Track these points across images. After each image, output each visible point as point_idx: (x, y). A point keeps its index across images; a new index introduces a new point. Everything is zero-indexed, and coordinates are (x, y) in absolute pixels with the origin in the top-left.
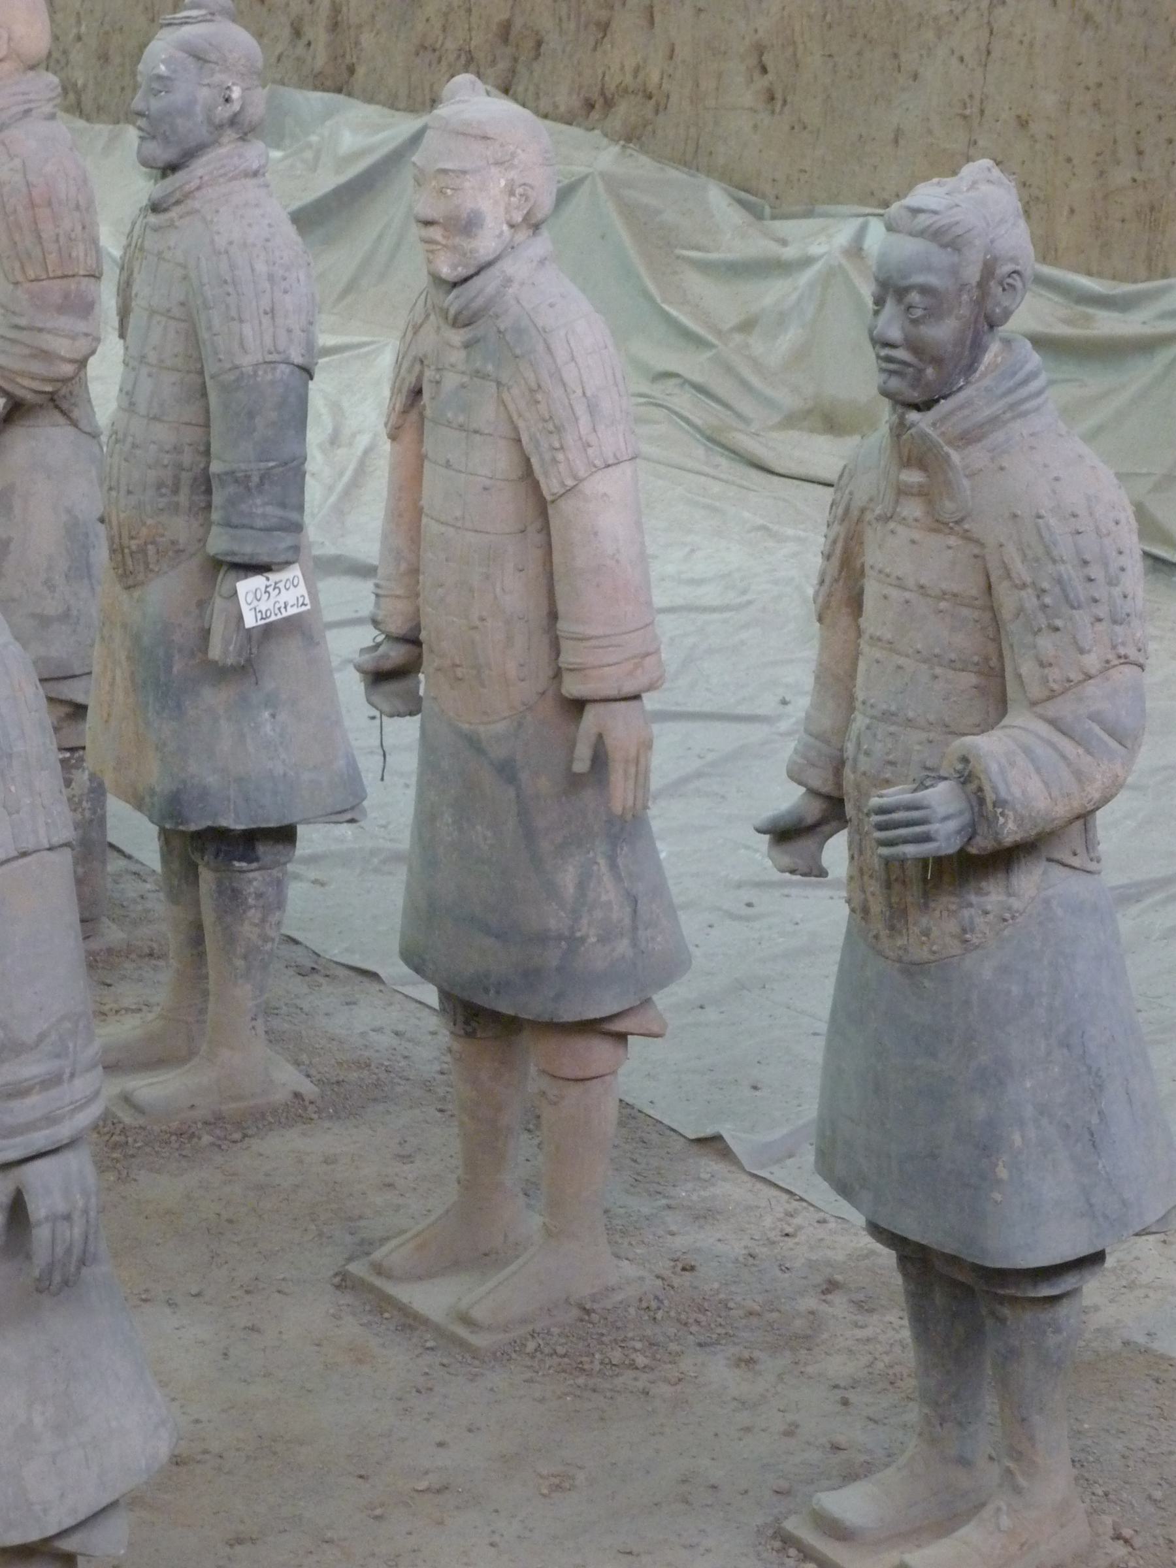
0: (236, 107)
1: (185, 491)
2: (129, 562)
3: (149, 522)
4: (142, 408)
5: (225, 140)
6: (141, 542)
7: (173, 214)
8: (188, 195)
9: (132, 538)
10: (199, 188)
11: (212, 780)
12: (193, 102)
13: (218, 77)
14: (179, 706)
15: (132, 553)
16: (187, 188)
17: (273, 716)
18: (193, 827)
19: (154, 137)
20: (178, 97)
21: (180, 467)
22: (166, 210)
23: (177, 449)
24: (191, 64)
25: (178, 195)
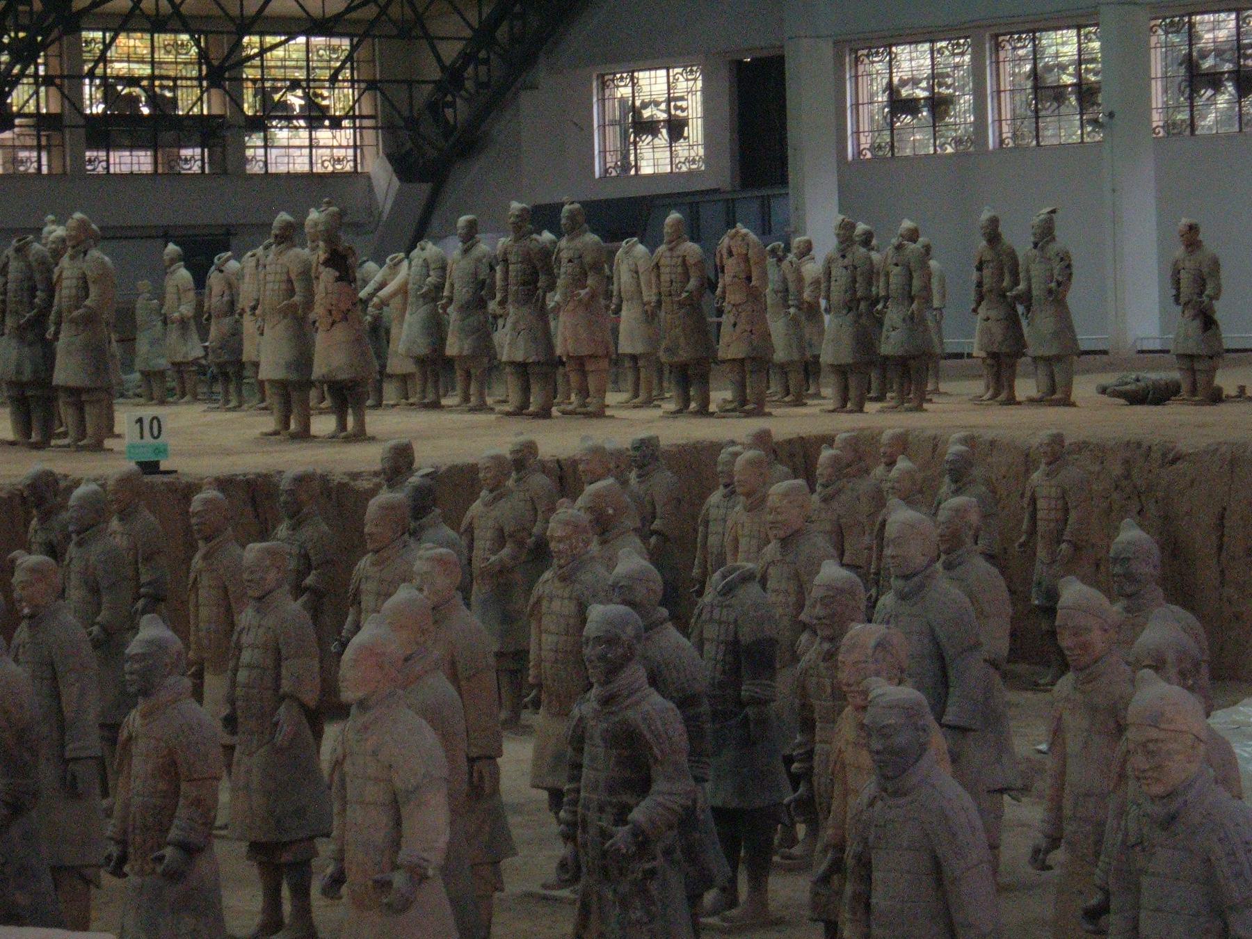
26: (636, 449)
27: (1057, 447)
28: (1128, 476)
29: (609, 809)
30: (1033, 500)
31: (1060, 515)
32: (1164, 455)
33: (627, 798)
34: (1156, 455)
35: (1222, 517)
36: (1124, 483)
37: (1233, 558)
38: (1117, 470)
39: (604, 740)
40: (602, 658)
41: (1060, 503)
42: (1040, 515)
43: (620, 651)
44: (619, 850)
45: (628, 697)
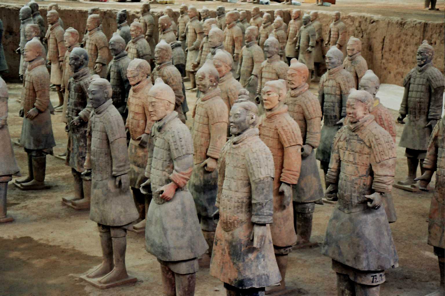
0: (253, 120)
1: (244, 207)
2: (229, 225)
3: (235, 215)
4: (233, 189)
5: (250, 127)
6: (232, 220)
7: (240, 144)
8: (243, 140)
9: (230, 219)
10: (246, 138)
11: (251, 276)
12: (245, 119)
13: (251, 113)
14: (243, 259)
15: (230, 223)
16: (243, 139)
17: (264, 260)
18: (247, 288)
19: (235, 127)
20: (242, 118)
21: (243, 202)
22: (237, 144)
23: (242, 198)
24: (245, 111)
25: (241, 140)
26: (218, 10)
27: (338, 16)
28: (360, 26)
29: (74, 111)
30: (330, 32)
31: (337, 36)
32: (370, 20)
33: (79, 108)
34: (368, 20)
35: (384, 40)
36: (359, 28)
37: (386, 51)
38: (357, 24)
39: (74, 90)
40: (73, 64)
41: (337, 33)
42: (332, 36)
43: (79, 62)
44: (74, 124)
45: (82, 76)
